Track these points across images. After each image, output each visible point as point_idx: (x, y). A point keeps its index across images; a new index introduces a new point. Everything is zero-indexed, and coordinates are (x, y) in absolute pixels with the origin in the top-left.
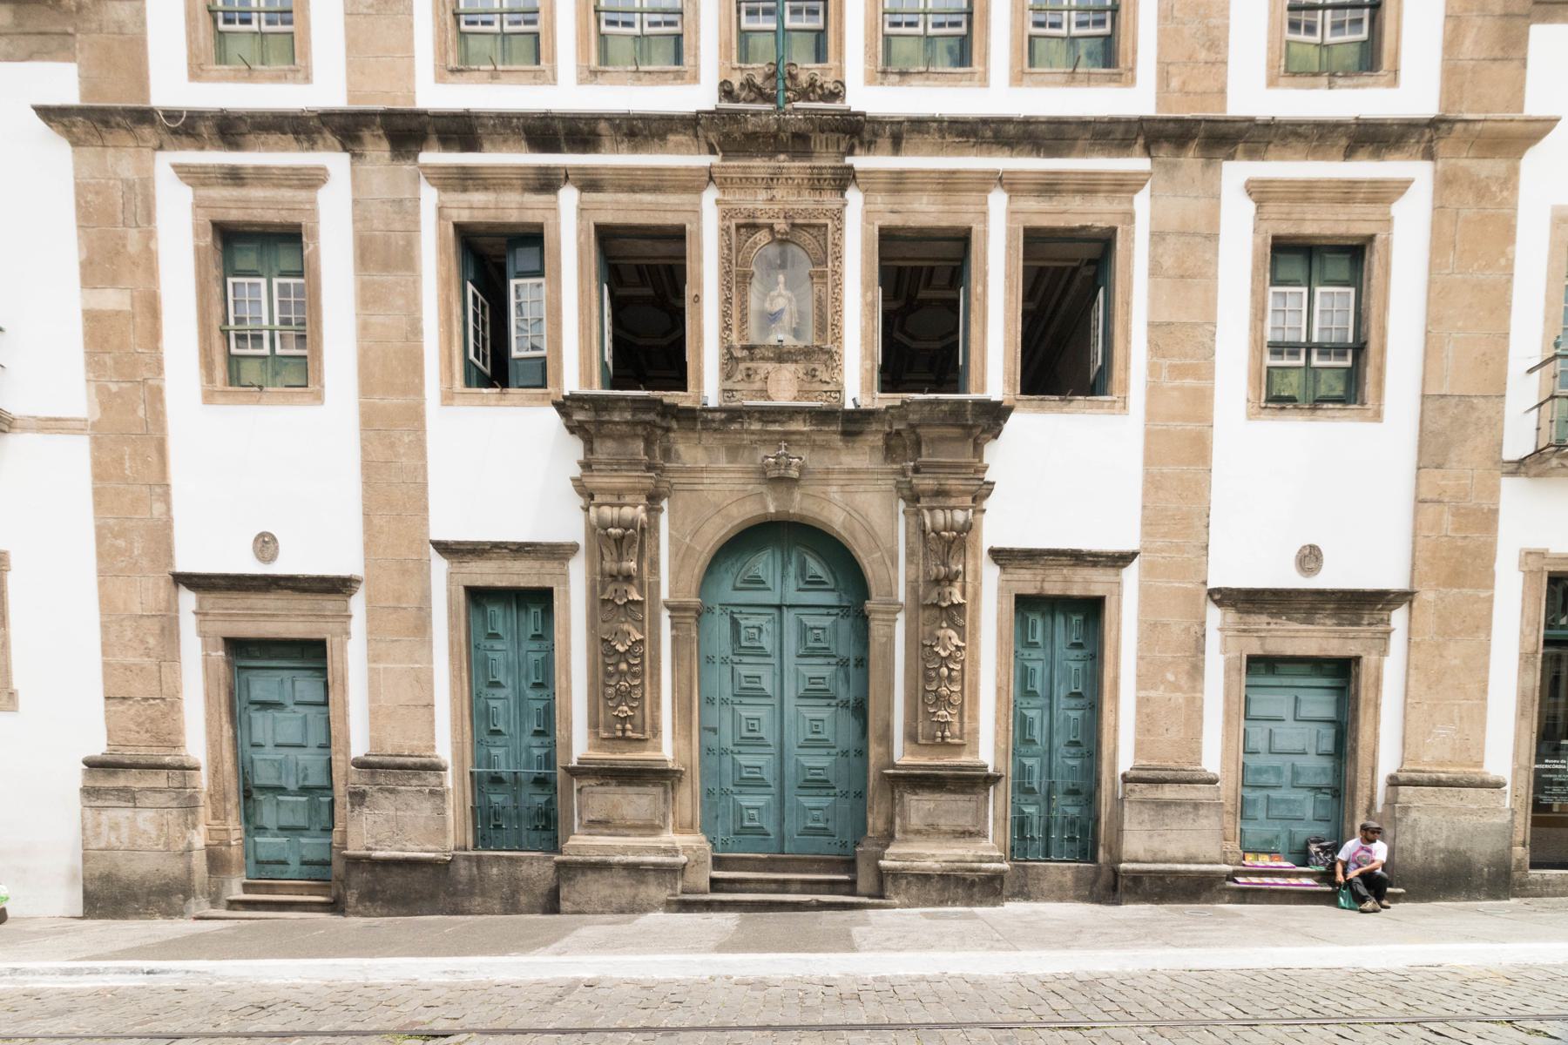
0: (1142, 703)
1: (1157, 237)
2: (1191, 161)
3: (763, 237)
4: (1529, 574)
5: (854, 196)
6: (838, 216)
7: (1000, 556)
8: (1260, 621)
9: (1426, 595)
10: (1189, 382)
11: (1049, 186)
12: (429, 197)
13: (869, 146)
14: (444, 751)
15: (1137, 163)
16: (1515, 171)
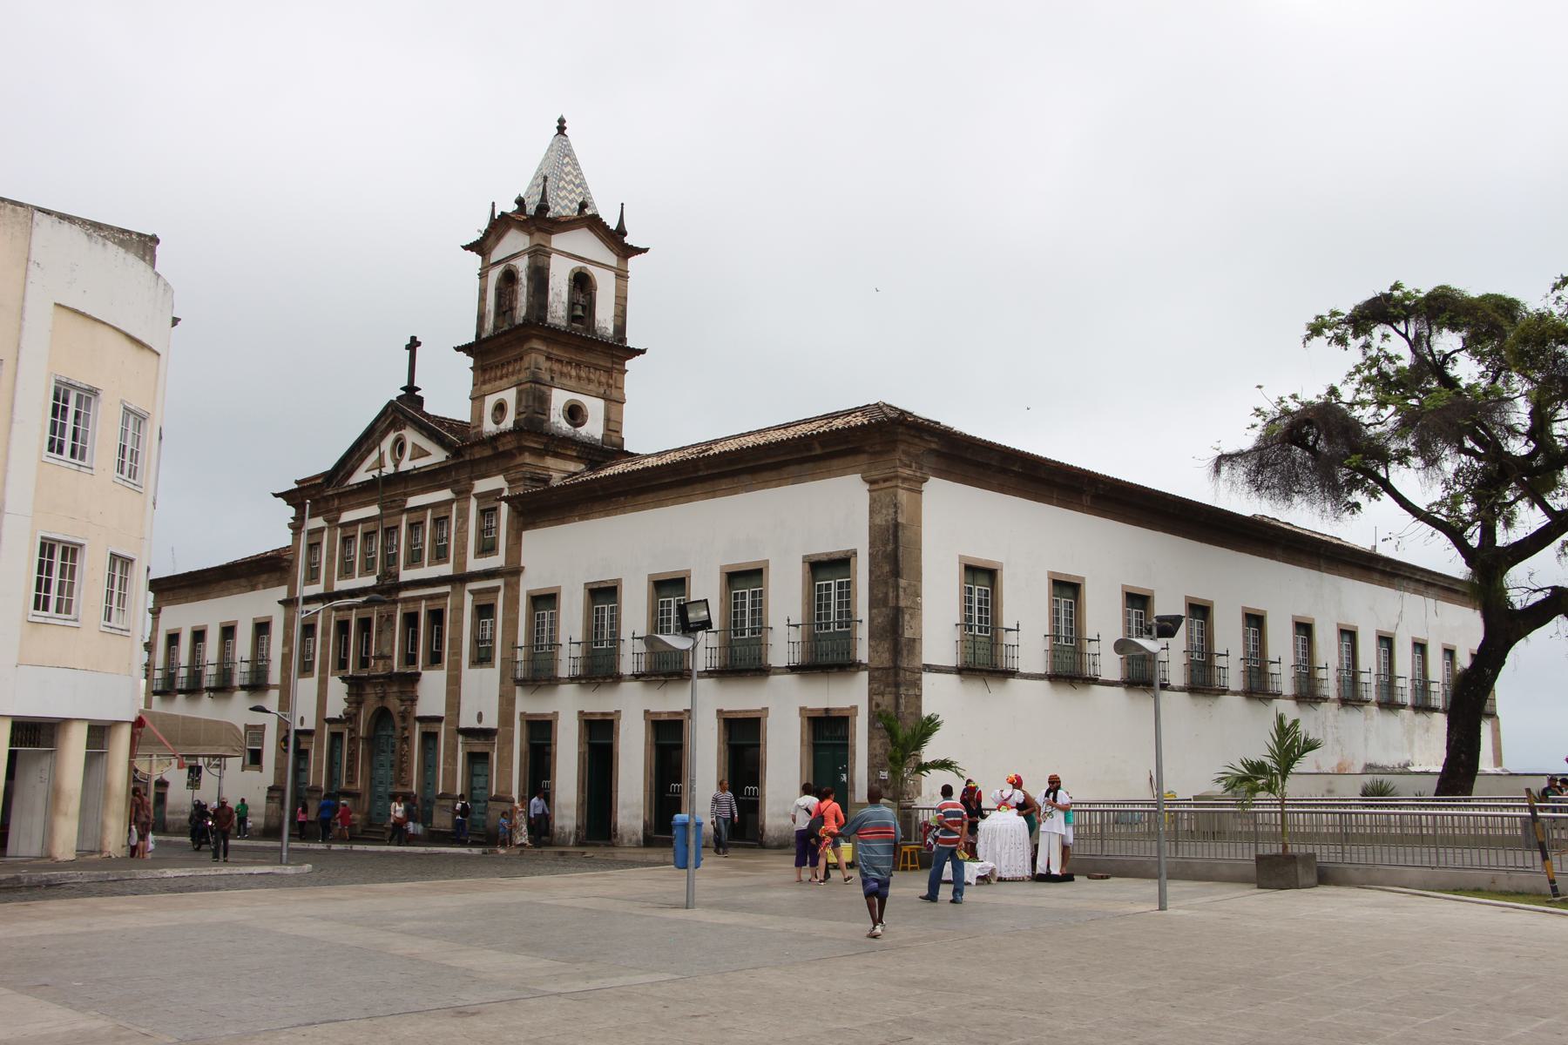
0: (444, 769)
1: (451, 610)
2: (458, 585)
3: (384, 619)
4: (521, 720)
5: (399, 605)
6: (396, 612)
7: (422, 720)
8: (470, 740)
9: (500, 730)
10: (456, 658)
11: (430, 598)
12: (334, 613)
13: (402, 590)
14: (323, 786)
15: (447, 589)
16: (519, 580)
